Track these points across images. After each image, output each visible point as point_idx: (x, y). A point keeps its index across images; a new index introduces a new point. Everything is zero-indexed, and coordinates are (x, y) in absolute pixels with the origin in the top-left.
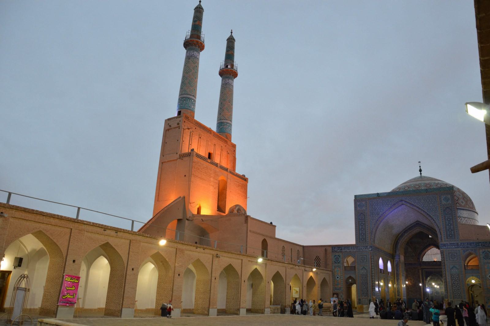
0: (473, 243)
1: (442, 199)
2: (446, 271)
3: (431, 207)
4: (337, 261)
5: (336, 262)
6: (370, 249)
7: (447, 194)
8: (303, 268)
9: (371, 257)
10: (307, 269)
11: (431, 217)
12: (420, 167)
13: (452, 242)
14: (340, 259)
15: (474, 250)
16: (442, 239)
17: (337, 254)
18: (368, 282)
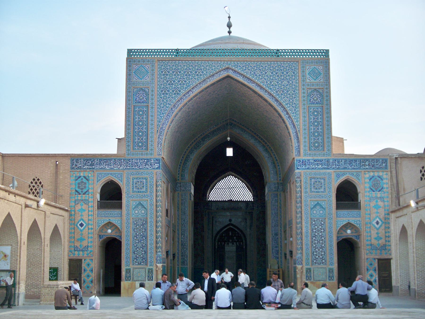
0: (356, 161)
1: (307, 72)
2: (303, 212)
3: (284, 85)
4: (82, 189)
5: (80, 191)
6: (156, 166)
7: (317, 62)
8: (22, 201)
9: (156, 182)
10: (29, 202)
11: (283, 107)
12: (229, 17)
13: (320, 158)
14: (87, 185)
15: (355, 174)
16: (299, 152)
17: (82, 174)
18: (149, 234)
